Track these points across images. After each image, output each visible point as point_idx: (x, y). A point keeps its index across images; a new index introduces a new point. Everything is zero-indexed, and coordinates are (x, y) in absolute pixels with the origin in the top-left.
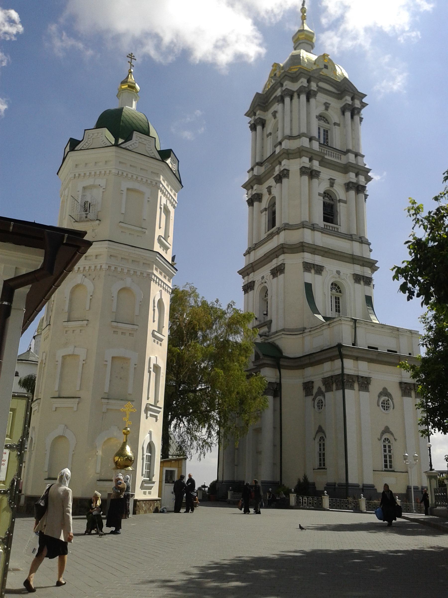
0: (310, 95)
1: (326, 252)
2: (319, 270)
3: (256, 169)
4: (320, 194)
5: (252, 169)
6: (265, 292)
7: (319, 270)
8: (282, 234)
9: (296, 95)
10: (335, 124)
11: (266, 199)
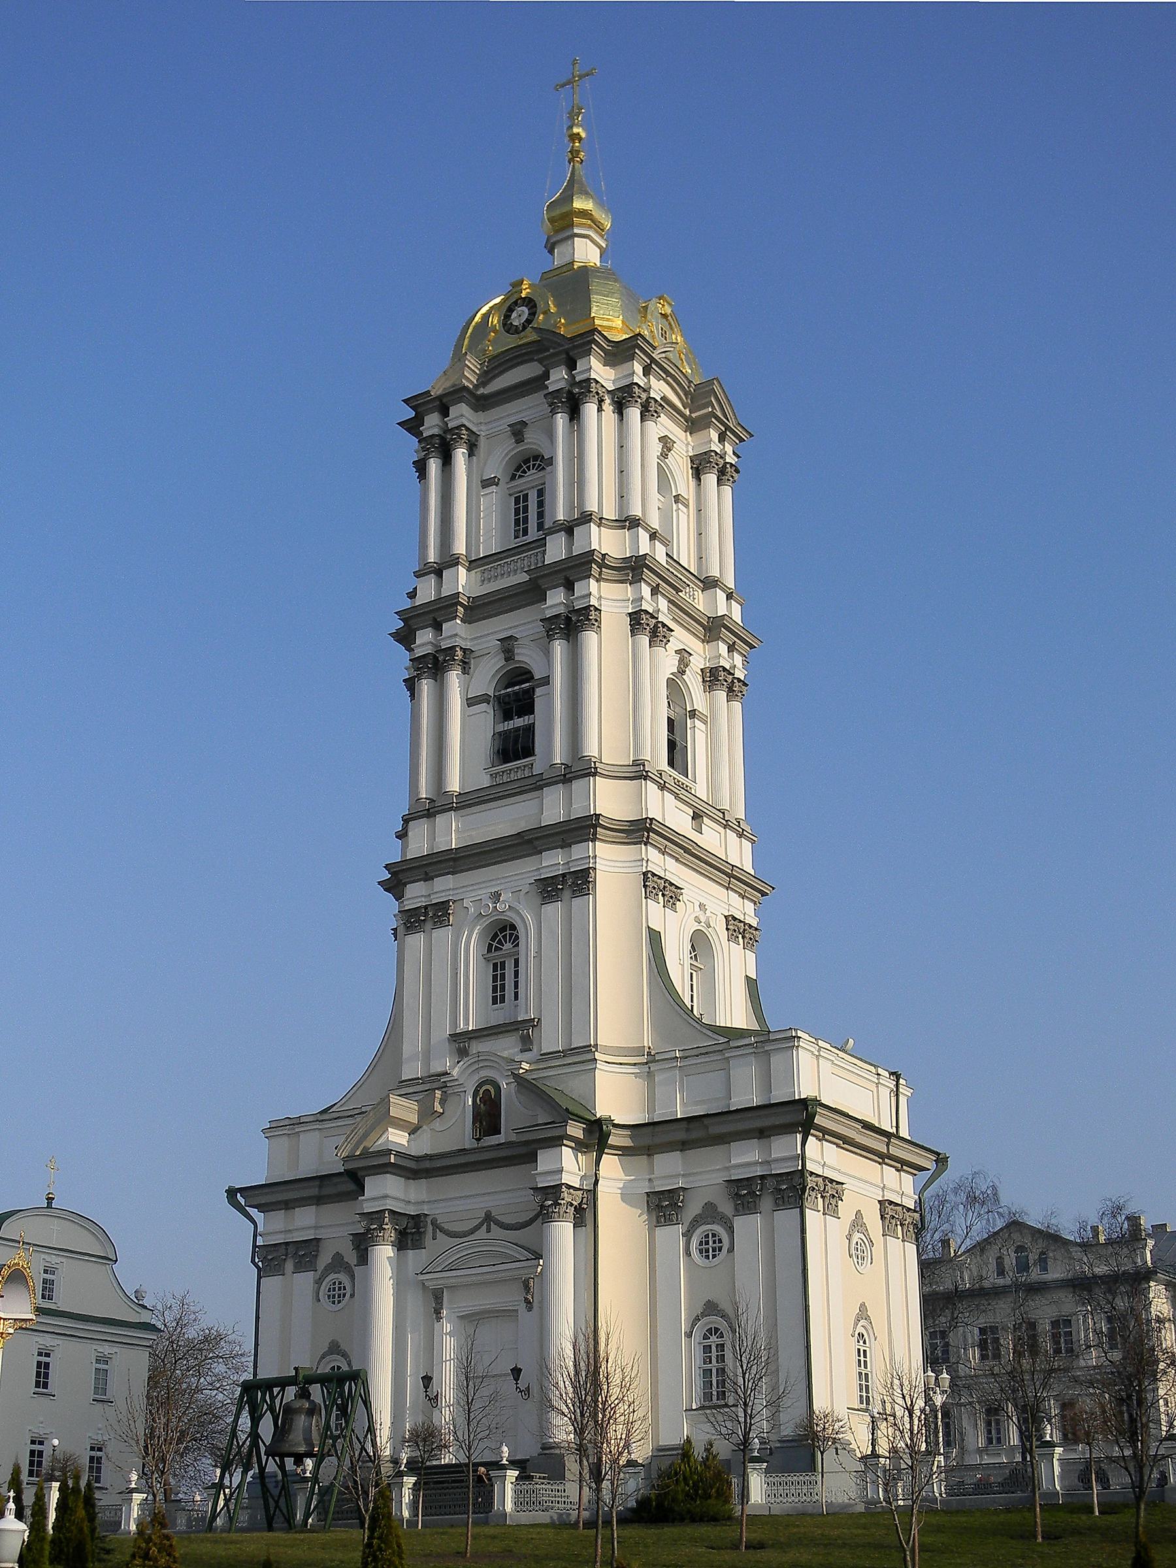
1: (686, 850)
6: (502, 935)
10: (677, 499)
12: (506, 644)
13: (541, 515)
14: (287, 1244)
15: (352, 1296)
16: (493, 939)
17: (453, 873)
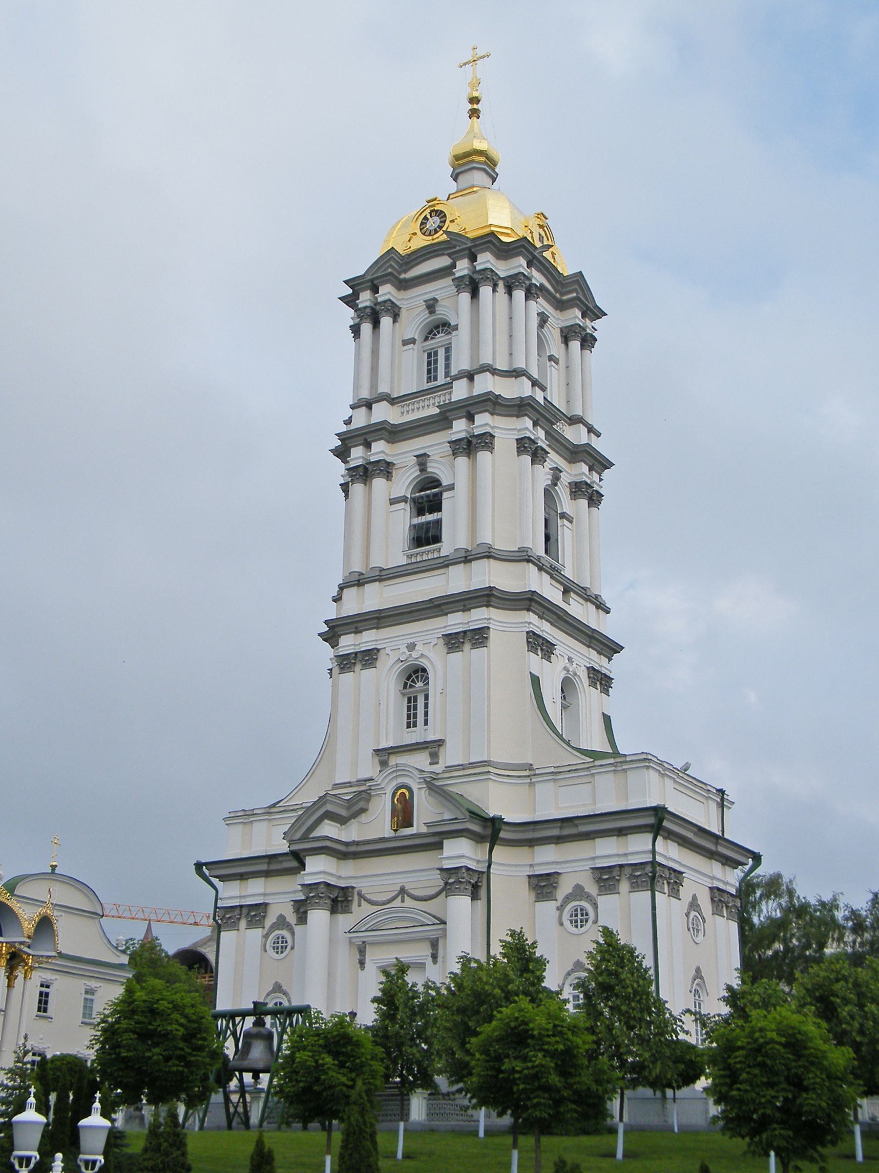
12: (420, 459)
13: (447, 366)
14: (241, 906)
15: (293, 948)
16: (408, 679)
17: (377, 628)
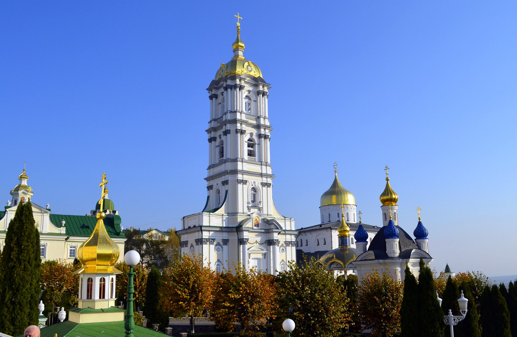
0: (241, 88)
2: (244, 182)
3: (213, 122)
4: (246, 142)
5: (210, 122)
6: (218, 192)
7: (244, 182)
8: (227, 164)
9: (233, 88)
11: (218, 140)
